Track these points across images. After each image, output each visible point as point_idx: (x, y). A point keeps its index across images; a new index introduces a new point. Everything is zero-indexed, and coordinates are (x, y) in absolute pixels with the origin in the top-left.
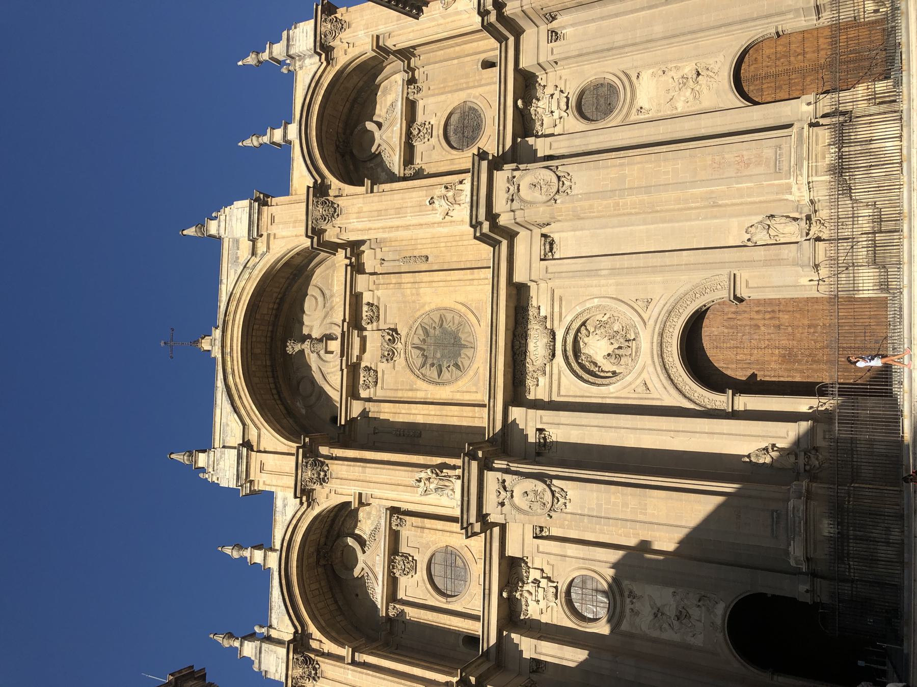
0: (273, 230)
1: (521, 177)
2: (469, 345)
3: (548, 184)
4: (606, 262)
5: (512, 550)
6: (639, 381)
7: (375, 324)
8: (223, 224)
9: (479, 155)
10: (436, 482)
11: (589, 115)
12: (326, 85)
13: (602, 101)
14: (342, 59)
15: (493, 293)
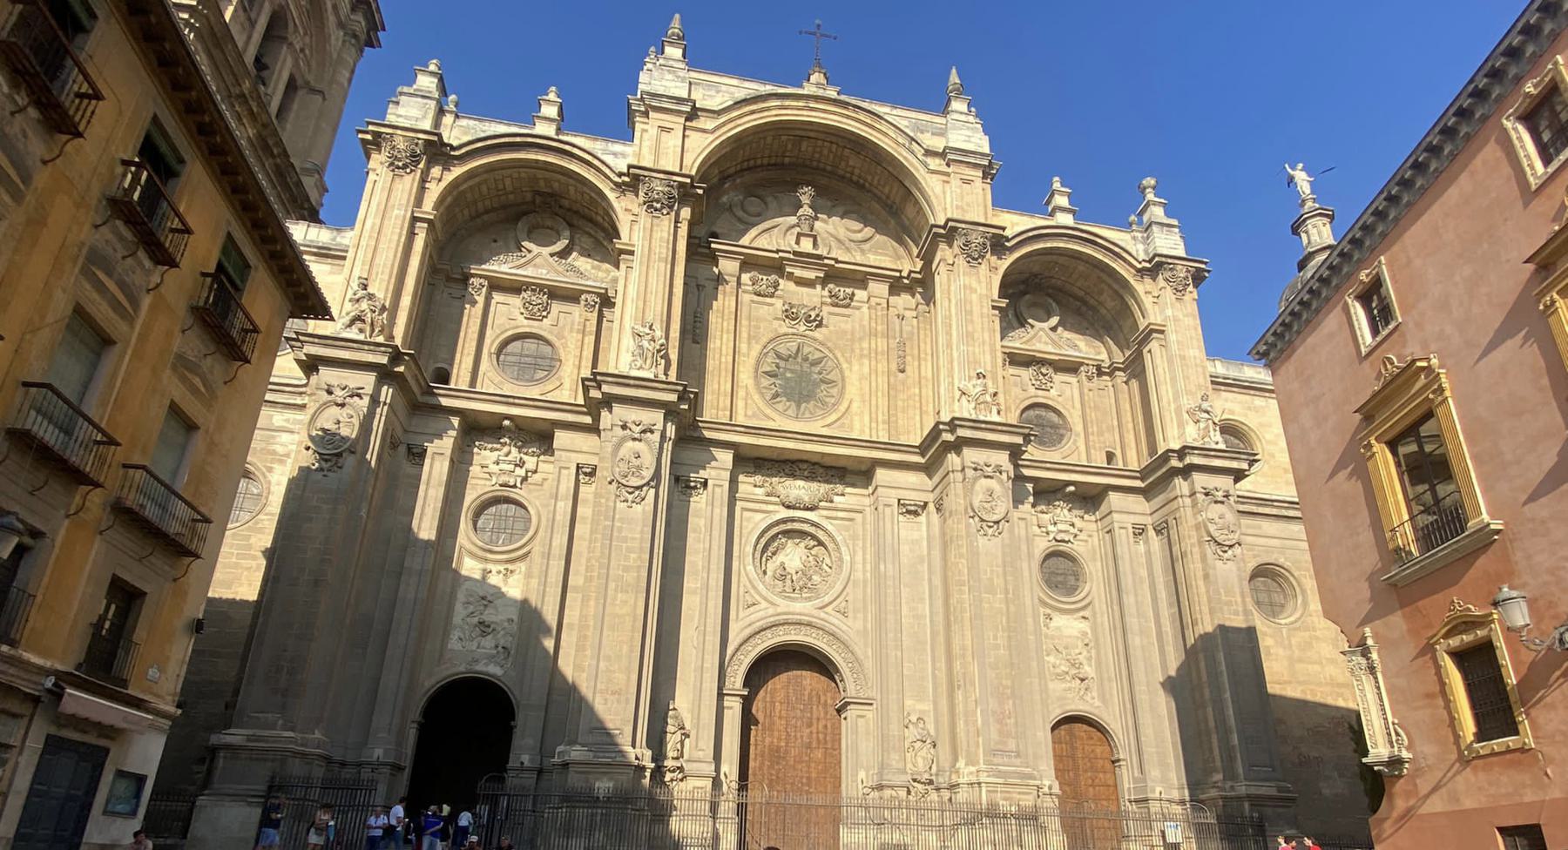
1: (1001, 482)
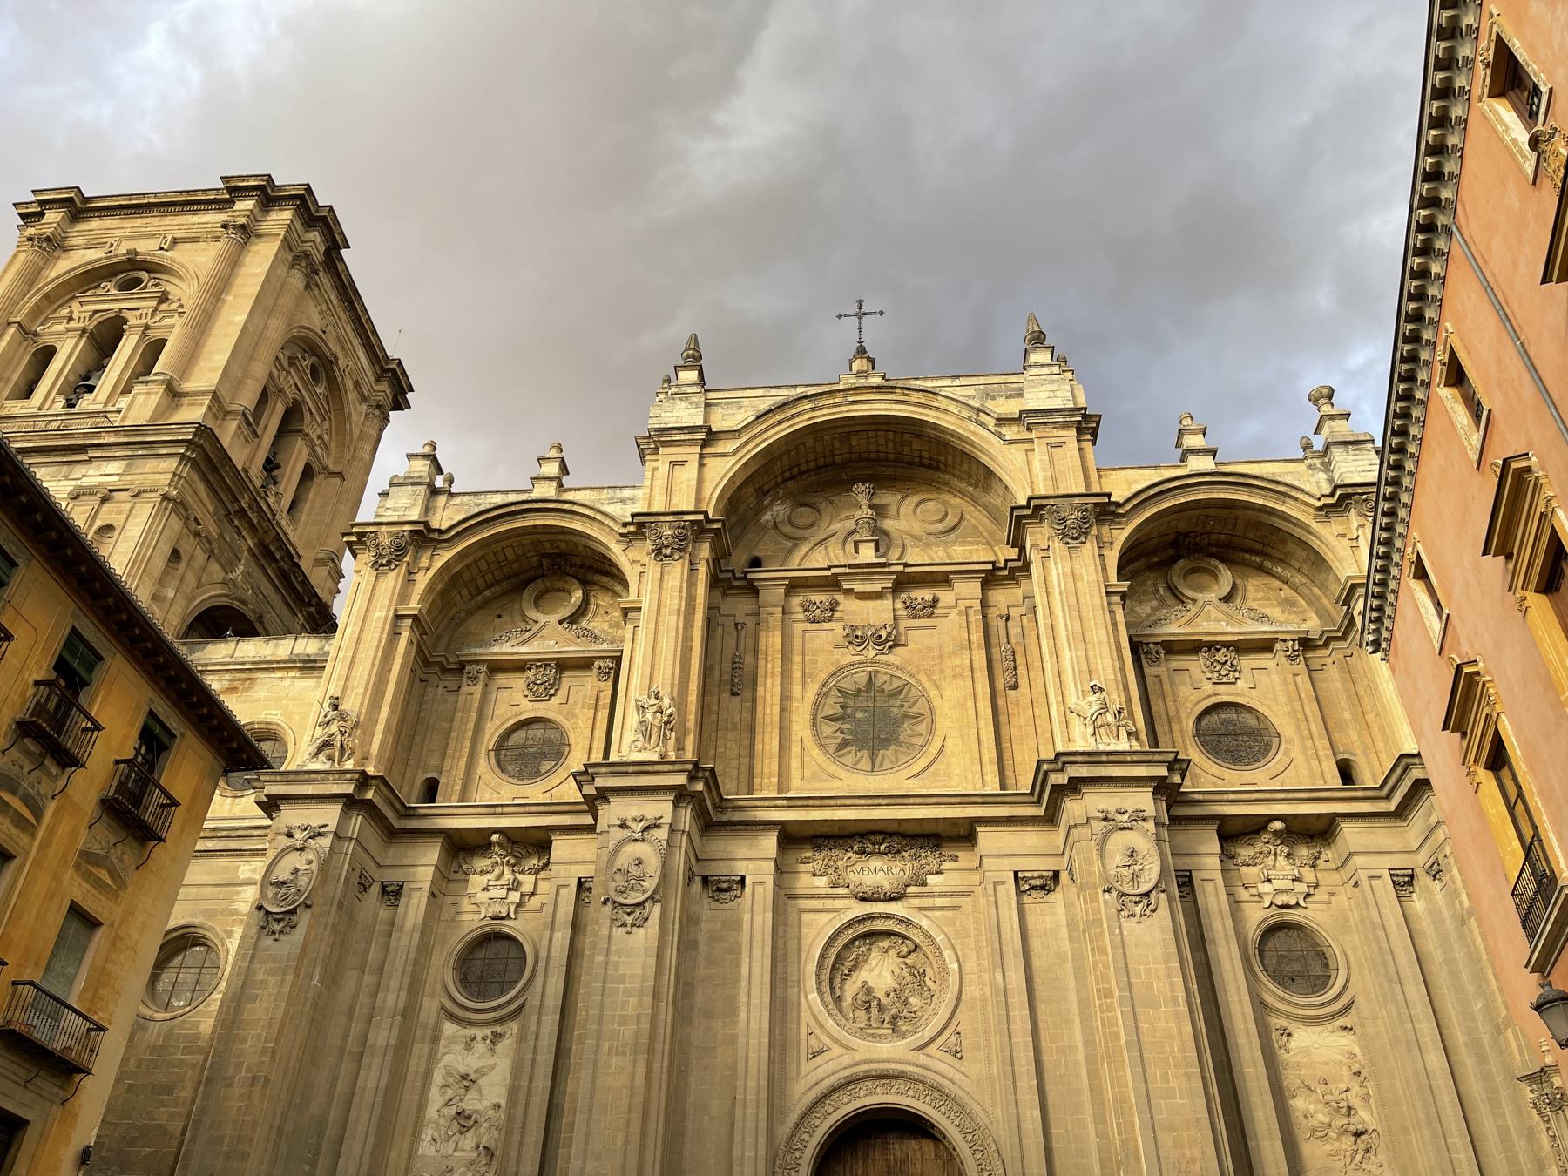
0: (1040, 448)
2: (877, 763)
3: (1135, 878)
4: (1017, 979)
5: (562, 847)
6: (827, 1041)
7: (904, 613)
8: (1045, 370)
9: (1176, 760)
10: (656, 722)
11: (1270, 944)
12: (1282, 508)
13: (1297, 967)
15: (956, 796)
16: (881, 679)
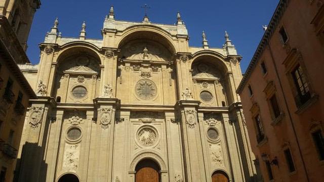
0: (180, 42)
14: (225, 63)
16: (147, 82)
